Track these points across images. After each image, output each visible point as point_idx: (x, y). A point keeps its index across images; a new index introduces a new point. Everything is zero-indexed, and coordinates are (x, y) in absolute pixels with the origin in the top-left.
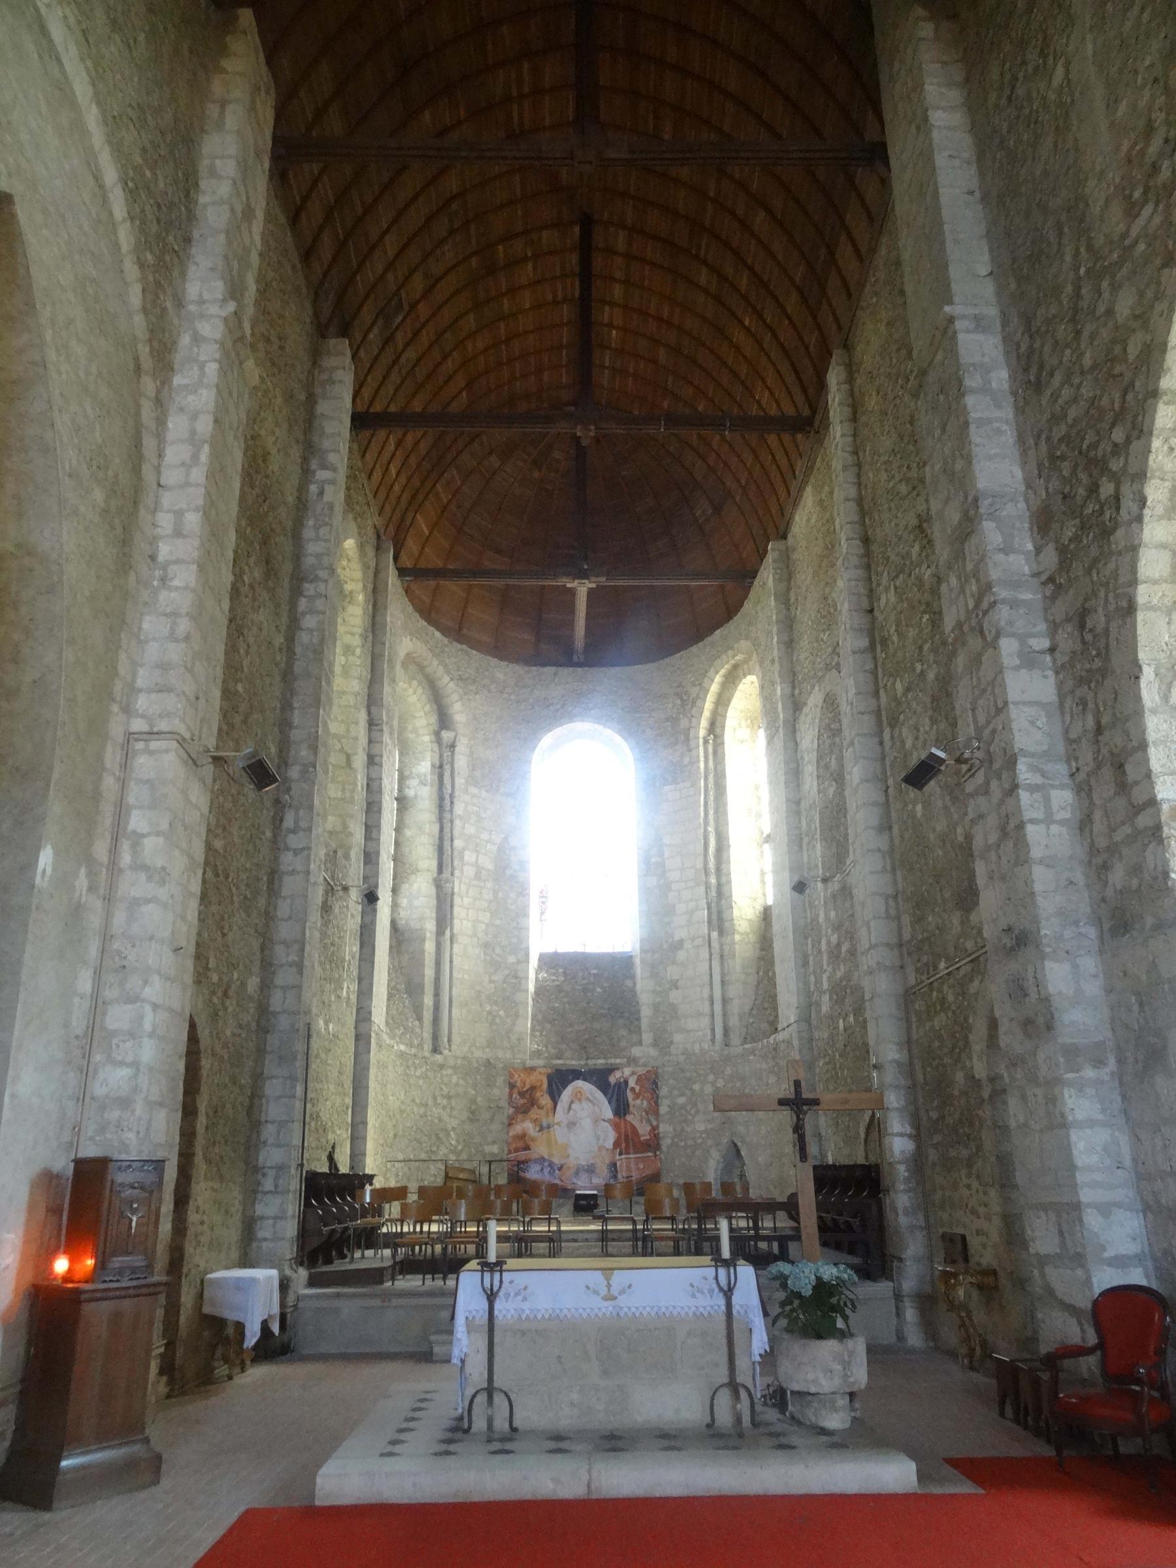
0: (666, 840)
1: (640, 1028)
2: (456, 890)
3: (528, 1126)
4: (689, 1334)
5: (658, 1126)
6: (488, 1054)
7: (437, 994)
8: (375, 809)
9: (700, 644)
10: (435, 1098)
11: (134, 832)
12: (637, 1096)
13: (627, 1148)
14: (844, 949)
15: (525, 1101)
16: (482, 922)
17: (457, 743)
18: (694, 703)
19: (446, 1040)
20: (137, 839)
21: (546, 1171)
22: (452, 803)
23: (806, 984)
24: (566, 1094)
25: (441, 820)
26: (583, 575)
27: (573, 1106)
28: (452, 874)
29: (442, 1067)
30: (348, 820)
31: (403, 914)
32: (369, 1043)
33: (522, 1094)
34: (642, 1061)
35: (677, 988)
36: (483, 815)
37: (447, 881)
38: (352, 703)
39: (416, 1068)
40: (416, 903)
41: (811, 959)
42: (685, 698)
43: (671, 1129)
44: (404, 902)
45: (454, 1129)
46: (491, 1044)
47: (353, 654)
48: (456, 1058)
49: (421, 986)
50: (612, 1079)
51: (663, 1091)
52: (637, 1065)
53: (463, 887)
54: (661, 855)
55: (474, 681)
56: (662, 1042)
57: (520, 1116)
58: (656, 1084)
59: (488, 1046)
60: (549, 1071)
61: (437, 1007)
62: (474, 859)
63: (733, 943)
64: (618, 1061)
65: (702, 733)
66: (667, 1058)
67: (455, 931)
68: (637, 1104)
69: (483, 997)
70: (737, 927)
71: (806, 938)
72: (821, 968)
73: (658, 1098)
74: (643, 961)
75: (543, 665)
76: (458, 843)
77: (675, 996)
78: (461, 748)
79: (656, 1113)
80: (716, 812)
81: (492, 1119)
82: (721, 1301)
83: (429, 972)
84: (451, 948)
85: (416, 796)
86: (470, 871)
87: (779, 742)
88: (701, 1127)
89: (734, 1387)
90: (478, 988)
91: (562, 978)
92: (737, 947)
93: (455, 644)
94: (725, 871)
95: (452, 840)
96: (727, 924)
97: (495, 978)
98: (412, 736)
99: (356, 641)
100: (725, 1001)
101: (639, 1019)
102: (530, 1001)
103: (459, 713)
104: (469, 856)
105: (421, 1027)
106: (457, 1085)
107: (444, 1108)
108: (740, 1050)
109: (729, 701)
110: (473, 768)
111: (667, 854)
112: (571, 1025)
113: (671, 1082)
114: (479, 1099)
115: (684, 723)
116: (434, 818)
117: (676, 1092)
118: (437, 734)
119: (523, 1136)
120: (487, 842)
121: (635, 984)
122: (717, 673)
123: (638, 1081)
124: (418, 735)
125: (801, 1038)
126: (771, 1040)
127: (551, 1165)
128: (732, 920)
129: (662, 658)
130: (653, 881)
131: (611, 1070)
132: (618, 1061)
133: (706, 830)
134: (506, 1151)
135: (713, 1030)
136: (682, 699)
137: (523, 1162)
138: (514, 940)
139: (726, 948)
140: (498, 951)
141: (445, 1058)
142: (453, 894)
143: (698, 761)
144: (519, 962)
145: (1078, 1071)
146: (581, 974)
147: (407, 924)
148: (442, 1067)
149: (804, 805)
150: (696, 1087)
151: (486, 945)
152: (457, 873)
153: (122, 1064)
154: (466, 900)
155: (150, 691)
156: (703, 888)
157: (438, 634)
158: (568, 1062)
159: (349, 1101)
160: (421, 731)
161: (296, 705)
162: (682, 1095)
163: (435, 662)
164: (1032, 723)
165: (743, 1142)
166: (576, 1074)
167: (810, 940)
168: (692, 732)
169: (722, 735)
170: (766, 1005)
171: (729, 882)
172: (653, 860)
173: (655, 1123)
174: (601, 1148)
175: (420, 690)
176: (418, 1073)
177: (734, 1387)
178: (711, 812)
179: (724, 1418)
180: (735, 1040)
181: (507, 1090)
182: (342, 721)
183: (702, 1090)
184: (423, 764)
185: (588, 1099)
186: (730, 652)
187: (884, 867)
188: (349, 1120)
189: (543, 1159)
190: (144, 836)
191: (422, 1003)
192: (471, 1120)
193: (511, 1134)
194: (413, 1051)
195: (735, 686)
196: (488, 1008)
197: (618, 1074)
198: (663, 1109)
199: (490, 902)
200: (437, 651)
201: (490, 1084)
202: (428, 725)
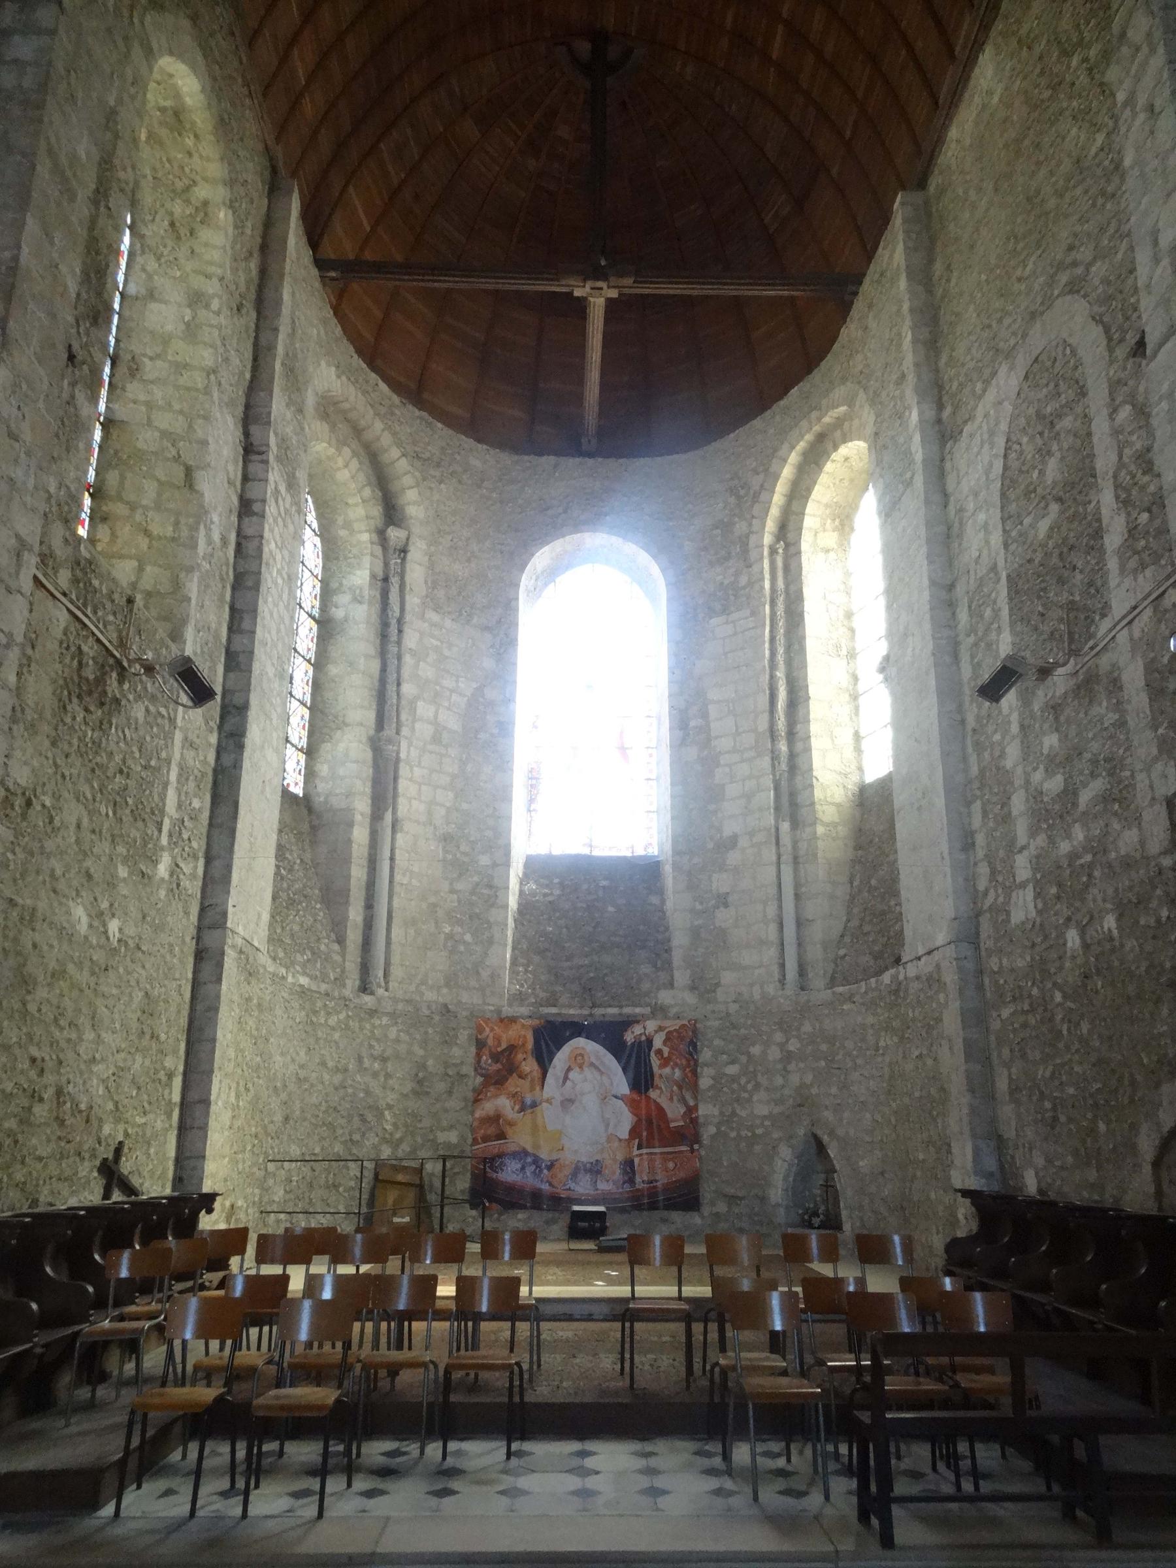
0: (713, 695)
1: (669, 963)
2: (403, 755)
3: (502, 1104)
5: (696, 1108)
6: (445, 996)
7: (369, 906)
8: (250, 583)
9: (768, 413)
10: (360, 1059)
12: (665, 1062)
13: (651, 1135)
14: (1085, 797)
15: (499, 1066)
16: (442, 805)
17: (411, 548)
18: (756, 498)
19: (381, 974)
21: (530, 1170)
22: (400, 631)
23: (971, 880)
25: (383, 654)
26: (598, 274)
27: (571, 1075)
28: (398, 733)
29: (373, 1013)
30: (182, 575)
31: (322, 787)
32: (220, 965)
33: (496, 1057)
34: (674, 1010)
35: (726, 905)
36: (446, 653)
37: (390, 741)
38: (200, 386)
39: (329, 1014)
40: (341, 771)
41: (980, 839)
42: (742, 492)
43: (716, 1112)
44: (323, 769)
45: (390, 1107)
46: (450, 981)
47: (207, 306)
48: (395, 1000)
49: (345, 893)
50: (629, 1037)
51: (705, 1055)
52: (666, 1017)
53: (414, 753)
54: (705, 715)
55: (438, 465)
56: (704, 986)
57: (492, 1089)
58: (695, 1046)
59: (447, 985)
60: (536, 1022)
61: (369, 924)
62: (431, 714)
63: (814, 836)
64: (638, 1010)
65: (767, 539)
66: (710, 1007)
67: (399, 814)
68: (665, 1074)
69: (440, 913)
70: (820, 815)
71: (968, 804)
72: (1012, 842)
74: (676, 866)
75: (540, 454)
76: (407, 689)
77: (723, 917)
78: (417, 553)
79: (694, 1087)
80: (788, 648)
81: (450, 1093)
83: (358, 873)
84: (393, 839)
85: (346, 619)
86: (424, 730)
87: (914, 502)
88: (762, 1110)
90: (432, 899)
91: (557, 892)
92: (820, 844)
93: (410, 407)
94: (801, 735)
95: (399, 684)
96: (804, 811)
97: (459, 886)
98: (343, 533)
99: (212, 287)
100: (799, 923)
101: (668, 951)
102: (511, 923)
103: (413, 503)
104: (424, 709)
105: (343, 954)
106: (398, 1041)
107: (375, 1075)
108: (826, 995)
109: (809, 491)
110: (435, 585)
112: (569, 958)
113: (717, 1042)
114: (430, 1062)
115: (740, 527)
116: (372, 651)
118: (381, 534)
119: (495, 1119)
121: (663, 902)
122: (793, 448)
123: (665, 1043)
124: (352, 532)
125: (961, 970)
126: (886, 978)
127: (537, 1161)
128: (813, 804)
129: (710, 443)
130: (692, 753)
131: (627, 1023)
132: (638, 1010)
133: (772, 677)
134: (470, 1141)
135: (782, 966)
136: (739, 498)
137: (493, 1159)
138: (489, 833)
139: (803, 846)
140: (464, 847)
141: (379, 1000)
142: (398, 760)
143: (763, 579)
144: (495, 865)
146: (585, 887)
147: (326, 802)
148: (373, 1013)
149: (960, 589)
150: (756, 1050)
151: (446, 839)
152: (405, 731)
154: (417, 772)
156: (766, 762)
157: (383, 386)
158: (564, 1011)
159: (176, 1063)
160: (356, 526)
162: (733, 1062)
163: (379, 425)
165: (832, 1133)
166: (577, 1029)
167: (977, 807)
168: (753, 539)
169: (797, 542)
170: (867, 928)
171: (808, 750)
172: (692, 724)
173: (692, 1103)
174: (610, 1139)
175: (354, 464)
176: (333, 1021)
178: (781, 650)
180: (818, 981)
181: (473, 1050)
182: (181, 412)
183: (764, 1053)
184: (358, 572)
185: (592, 1065)
186: (814, 414)
188: (176, 1097)
189: (525, 1153)
191: (345, 919)
192: (416, 1093)
193: (477, 1115)
194: (324, 987)
195: (819, 467)
196: (447, 929)
197: (638, 1030)
198: (705, 1082)
200: (383, 410)
201: (448, 1040)
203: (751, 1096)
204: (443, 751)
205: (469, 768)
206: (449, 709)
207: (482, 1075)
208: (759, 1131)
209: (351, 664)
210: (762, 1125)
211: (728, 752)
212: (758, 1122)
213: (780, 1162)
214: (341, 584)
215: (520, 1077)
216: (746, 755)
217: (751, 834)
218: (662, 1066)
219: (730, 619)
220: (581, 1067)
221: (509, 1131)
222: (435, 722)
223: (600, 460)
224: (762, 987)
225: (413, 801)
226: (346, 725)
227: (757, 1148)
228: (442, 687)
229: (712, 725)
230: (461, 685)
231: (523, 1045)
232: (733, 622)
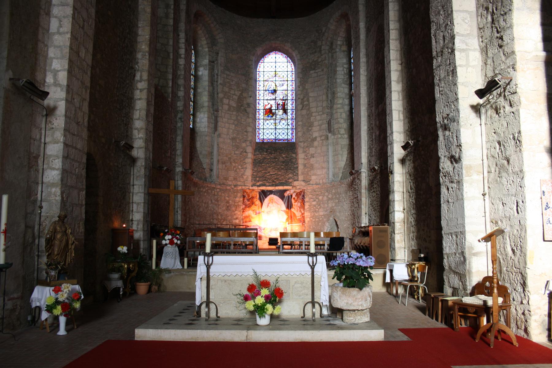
0: (311, 94)
1: (298, 173)
4: (296, 283)
5: (304, 213)
11: (54, 69)
15: (249, 202)
20: (55, 73)
24: (267, 200)
27: (270, 205)
35: (313, 157)
36: (231, 83)
40: (203, 120)
47: (170, 8)
51: (306, 199)
53: (223, 114)
54: (308, 100)
57: (247, 208)
73: (304, 202)
76: (221, 95)
82: (310, 270)
86: (226, 107)
88: (321, 213)
89: (313, 303)
90: (229, 156)
97: (237, 152)
98: (200, 48)
104: (226, 101)
111: (311, 100)
117: (312, 200)
120: (233, 95)
123: (296, 196)
131: (285, 191)
145: (470, 176)
147: (199, 129)
151: (233, 139)
153: (54, 169)
155: (58, 5)
161: (140, 25)
162: (314, 201)
164: (463, 20)
166: (271, 192)
177: (313, 303)
179: (309, 314)
184: (205, 61)
185: (276, 202)
187: (399, 98)
190: (58, 71)
197: (288, 192)
199: (234, 120)
202: (207, 44)
203: (319, 210)
204: (231, 113)
205: (239, 118)
206: (232, 100)
207: (245, 205)
208: (321, 219)
209: (204, 89)
210: (321, 217)
211: (314, 112)
212: (320, 217)
213: (326, 227)
214: (200, 64)
215: (255, 205)
216: (320, 113)
217: (321, 136)
218: (295, 202)
219: (316, 72)
220: (272, 202)
221: (252, 220)
222: (228, 105)
223: (277, 19)
224: (322, 180)
225: (223, 128)
226: (204, 107)
227: (320, 224)
228: (230, 94)
229: (310, 104)
230: (236, 93)
231: (256, 197)
232: (317, 73)
